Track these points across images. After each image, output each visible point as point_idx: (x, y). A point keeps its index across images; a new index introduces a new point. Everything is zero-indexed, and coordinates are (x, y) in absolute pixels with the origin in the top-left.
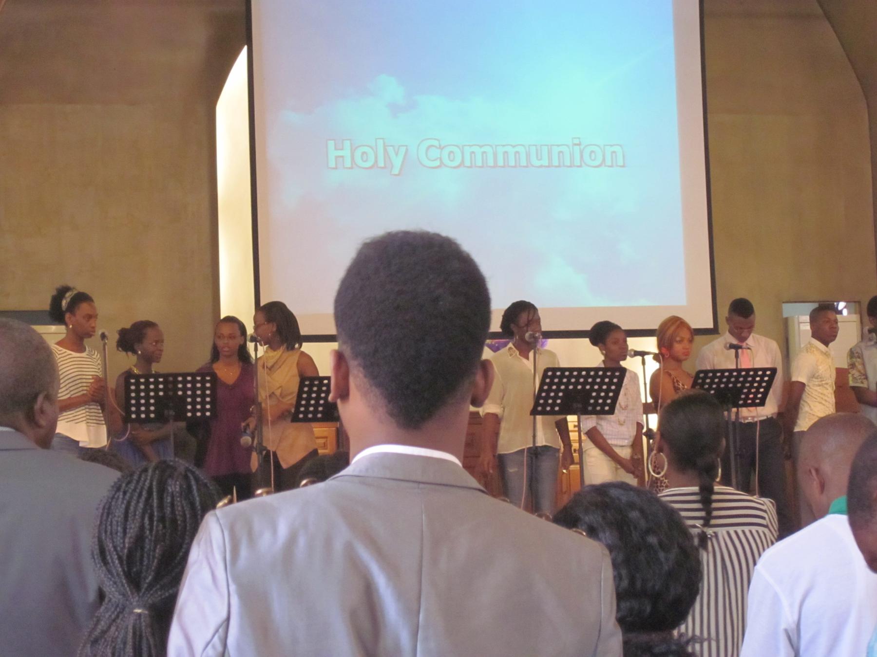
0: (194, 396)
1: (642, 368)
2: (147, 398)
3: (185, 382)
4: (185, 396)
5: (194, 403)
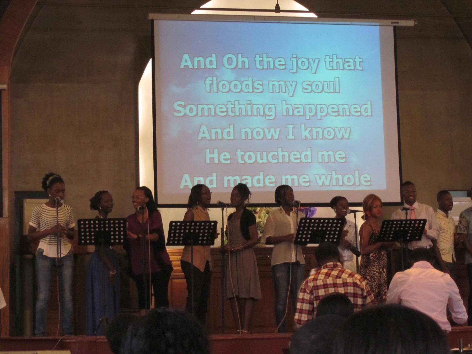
0: (114, 231)
1: (357, 219)
2: (90, 232)
4: (110, 231)
5: (115, 235)
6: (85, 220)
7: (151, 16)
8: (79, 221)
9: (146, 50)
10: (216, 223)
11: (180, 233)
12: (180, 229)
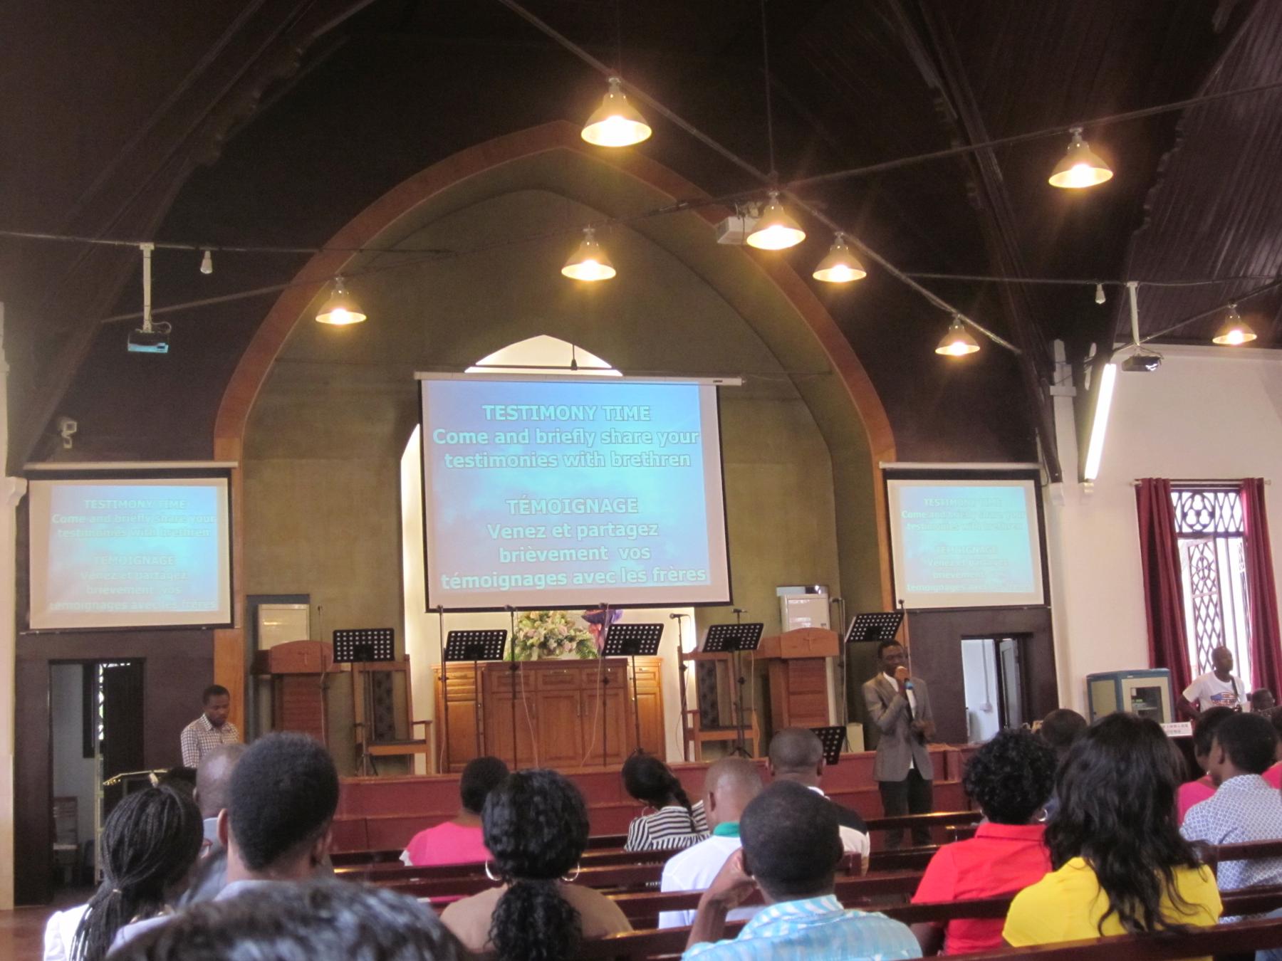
0: (379, 645)
2: (348, 646)
3: (373, 635)
4: (373, 644)
5: (379, 650)
6: (341, 632)
7: (418, 375)
8: (335, 633)
9: (411, 413)
10: (505, 632)
11: (461, 645)
12: (461, 641)
